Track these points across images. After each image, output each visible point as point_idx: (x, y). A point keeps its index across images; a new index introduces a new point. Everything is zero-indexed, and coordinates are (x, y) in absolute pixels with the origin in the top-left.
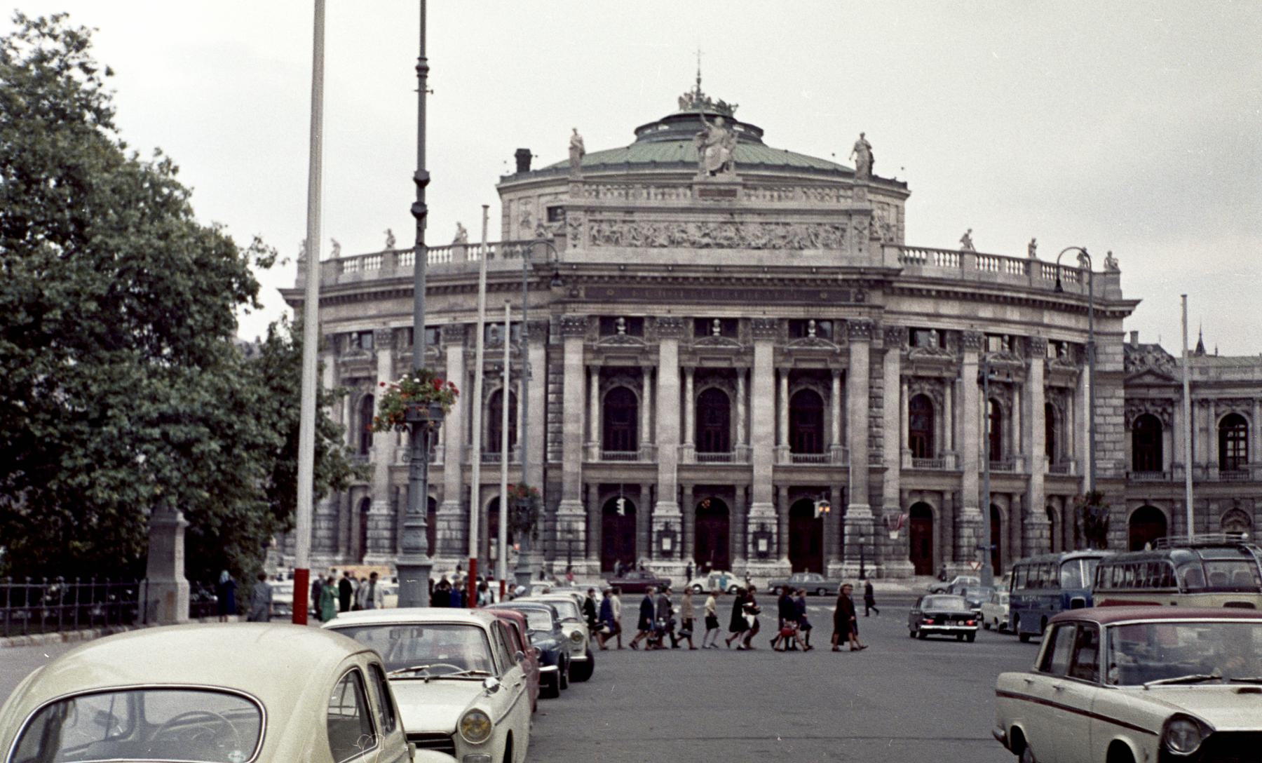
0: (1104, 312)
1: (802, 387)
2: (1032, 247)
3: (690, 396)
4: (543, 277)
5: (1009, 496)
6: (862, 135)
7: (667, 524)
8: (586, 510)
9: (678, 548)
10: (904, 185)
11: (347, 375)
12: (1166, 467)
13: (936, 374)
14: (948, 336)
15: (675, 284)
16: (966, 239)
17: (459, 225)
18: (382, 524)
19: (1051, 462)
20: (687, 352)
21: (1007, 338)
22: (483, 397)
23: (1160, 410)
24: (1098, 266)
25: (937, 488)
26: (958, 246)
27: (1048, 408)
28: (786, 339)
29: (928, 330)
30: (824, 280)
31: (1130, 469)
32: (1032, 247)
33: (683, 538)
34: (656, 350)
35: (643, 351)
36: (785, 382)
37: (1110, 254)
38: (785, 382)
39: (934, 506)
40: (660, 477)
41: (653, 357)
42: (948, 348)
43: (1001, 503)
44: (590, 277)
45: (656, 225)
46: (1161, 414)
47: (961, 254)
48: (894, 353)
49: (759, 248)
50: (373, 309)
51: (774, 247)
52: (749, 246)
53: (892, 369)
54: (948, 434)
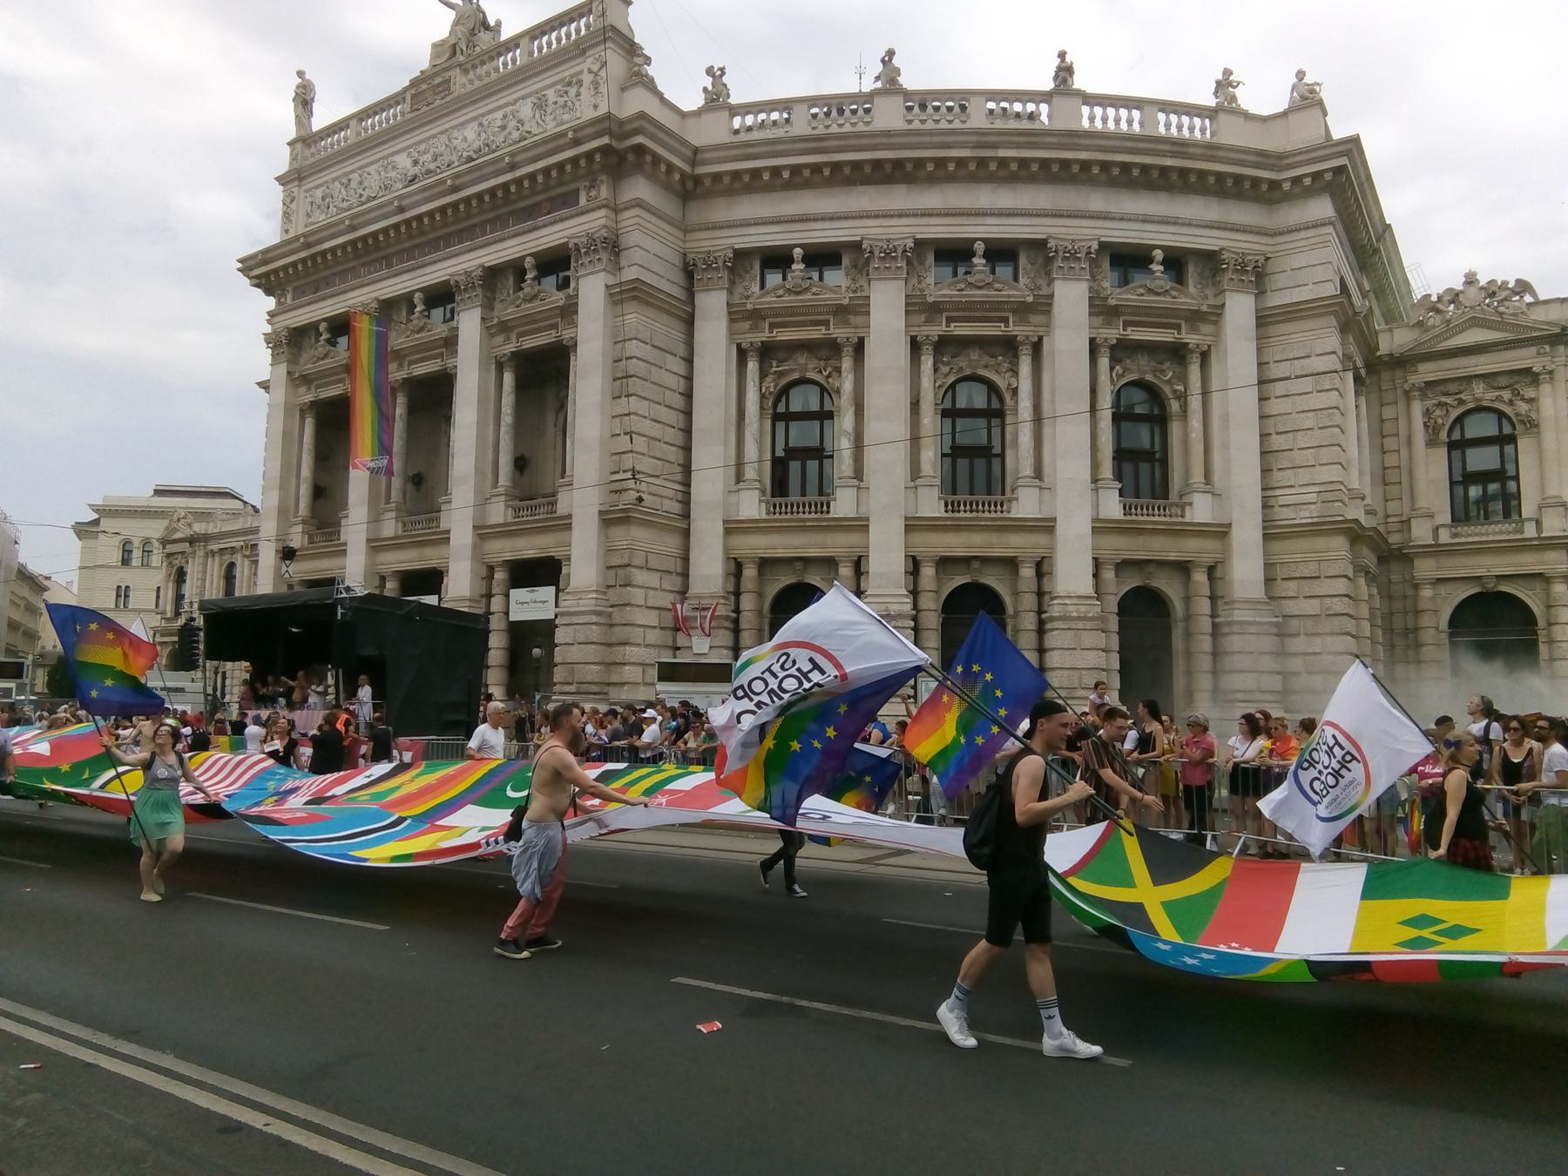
0: (1274, 185)
2: (1064, 72)
12: (1528, 509)
37: (1301, 75)
46: (1511, 403)
48: (713, 305)
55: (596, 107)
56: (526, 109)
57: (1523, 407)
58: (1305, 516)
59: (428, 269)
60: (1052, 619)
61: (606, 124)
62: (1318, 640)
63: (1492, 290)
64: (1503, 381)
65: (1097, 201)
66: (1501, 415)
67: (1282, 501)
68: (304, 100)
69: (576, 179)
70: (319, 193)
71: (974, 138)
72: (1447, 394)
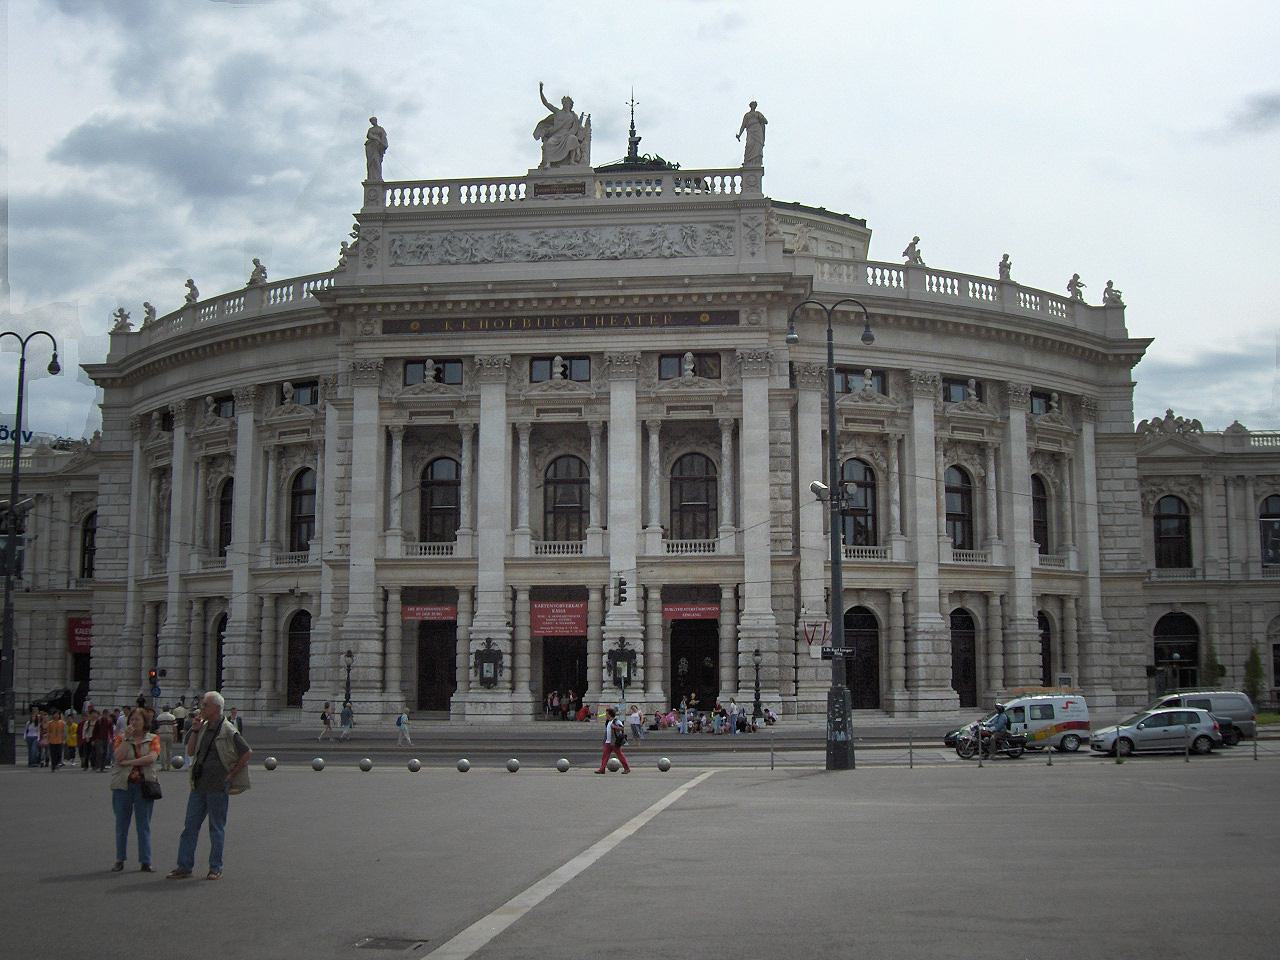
0: (1105, 356)
1: (687, 450)
2: (1005, 267)
3: (524, 462)
4: (329, 310)
5: (985, 597)
6: (753, 105)
7: (489, 640)
8: (385, 625)
9: (506, 674)
10: (863, 223)
11: (152, 466)
12: (1196, 562)
13: (875, 429)
14: (891, 380)
15: (499, 313)
16: (912, 251)
17: (256, 262)
18: (172, 648)
19: (1043, 550)
20: (519, 403)
21: (972, 382)
22: (278, 478)
23: (1186, 489)
24: (1094, 297)
25: (879, 586)
26: (903, 261)
27: (1037, 479)
28: (656, 379)
29: (859, 371)
30: (702, 296)
31: (1152, 565)
32: (1005, 267)
33: (513, 661)
34: (476, 402)
35: (461, 405)
36: (654, 439)
37: (1110, 284)
38: (654, 439)
39: (879, 613)
40: (502, 573)
41: (472, 411)
42: (892, 395)
43: (974, 607)
44: (387, 305)
45: (477, 235)
46: (1188, 495)
47: (905, 268)
49: (616, 258)
50: (173, 378)
51: (636, 256)
52: (602, 257)
53: (812, 424)
54: (895, 511)
55: (753, 254)
56: (674, 234)
57: (1195, 499)
58: (1123, 568)
59: (571, 340)
60: (1016, 634)
61: (788, 279)
62: (1129, 646)
63: (1180, 423)
64: (1183, 480)
65: (1028, 358)
66: (1181, 500)
67: (1107, 557)
68: (376, 144)
69: (739, 303)
70: (410, 241)
71: (978, 314)
72: (1154, 485)
